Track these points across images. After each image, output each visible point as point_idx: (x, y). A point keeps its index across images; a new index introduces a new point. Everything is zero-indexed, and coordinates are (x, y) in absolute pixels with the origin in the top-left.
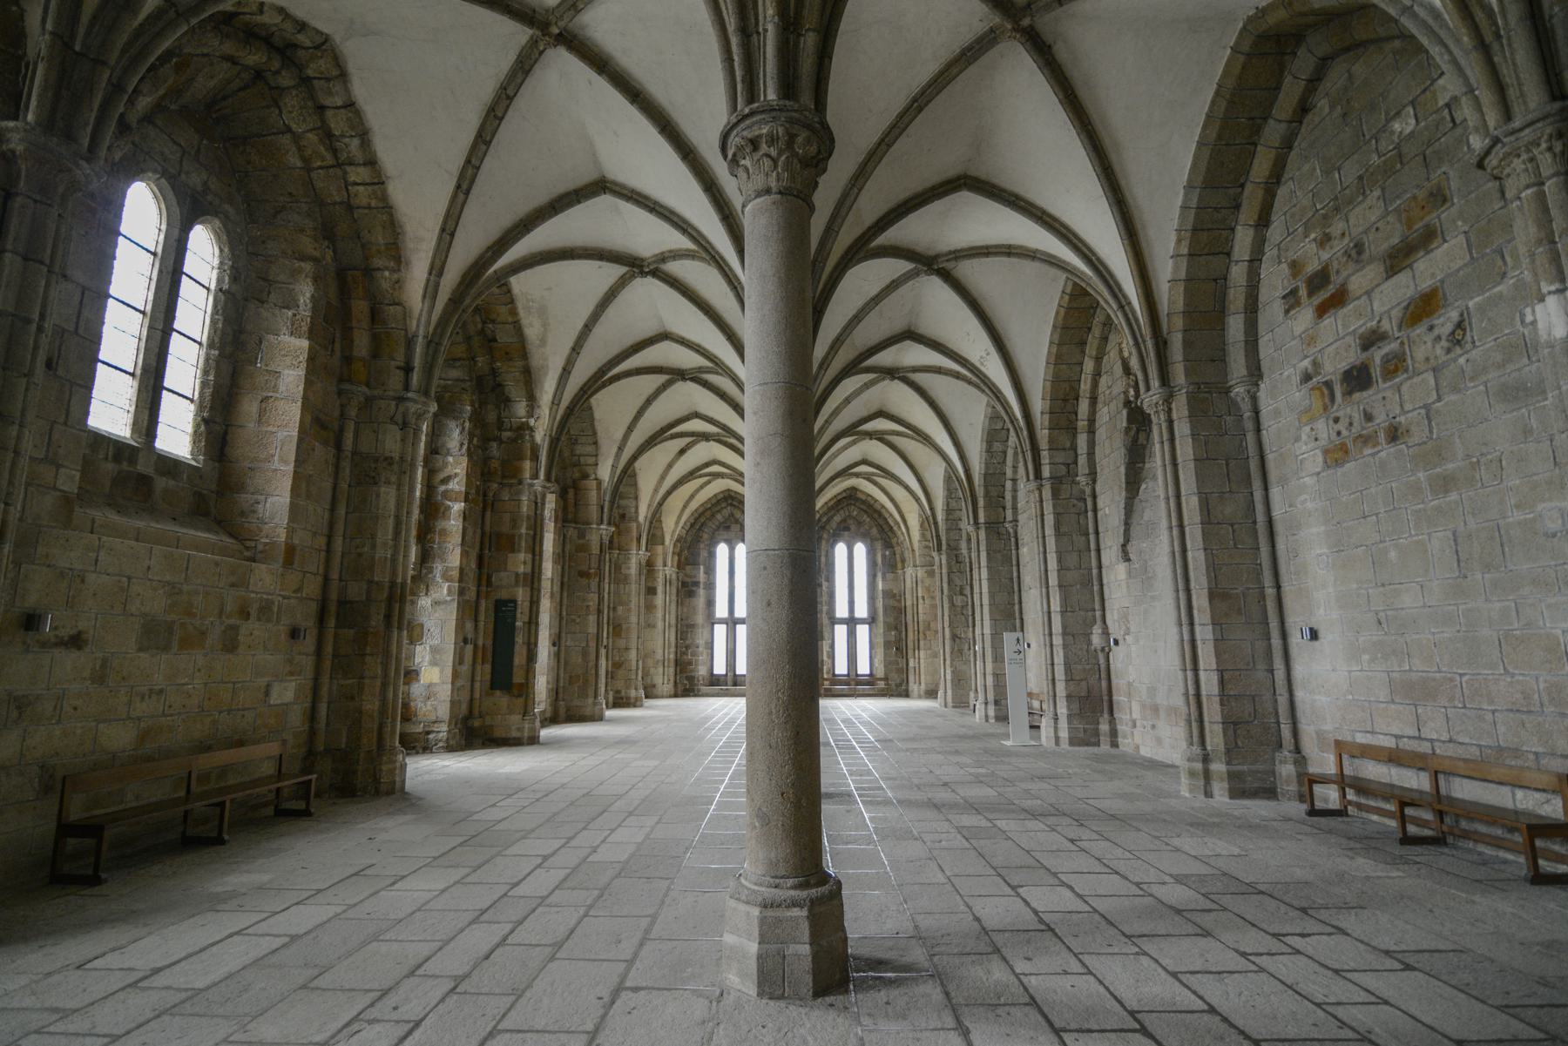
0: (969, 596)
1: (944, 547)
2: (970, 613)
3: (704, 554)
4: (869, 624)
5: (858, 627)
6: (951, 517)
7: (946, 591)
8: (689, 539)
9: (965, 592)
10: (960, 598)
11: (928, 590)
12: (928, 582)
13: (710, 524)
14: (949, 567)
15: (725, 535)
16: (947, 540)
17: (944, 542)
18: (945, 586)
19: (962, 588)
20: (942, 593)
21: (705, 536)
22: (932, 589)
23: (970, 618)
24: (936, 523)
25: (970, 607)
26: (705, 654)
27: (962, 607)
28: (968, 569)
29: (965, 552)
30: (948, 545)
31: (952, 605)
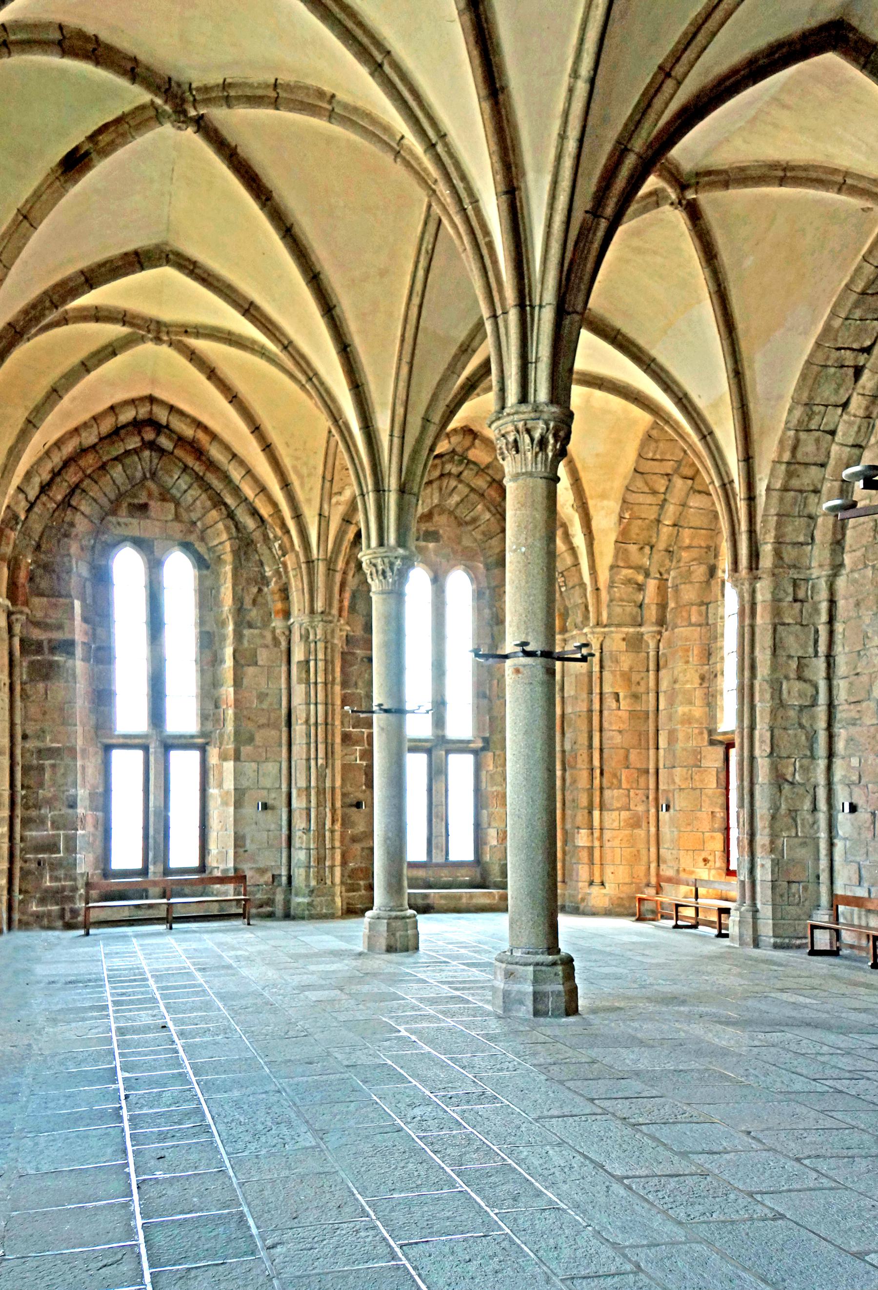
0: (822, 685)
1: (767, 561)
2: (822, 724)
3: (80, 569)
4: (476, 752)
5: (453, 758)
6: (795, 483)
7: (763, 670)
8: (37, 528)
9: (807, 674)
10: (797, 686)
11: (627, 677)
12: (626, 661)
13: (94, 491)
14: (777, 612)
15: (136, 526)
16: (779, 543)
17: (767, 550)
18: (763, 657)
19: (802, 664)
20: (753, 676)
21: (82, 525)
22: (635, 677)
23: (822, 737)
24: (751, 499)
25: (821, 711)
26: (90, 828)
27: (802, 708)
28: (824, 617)
29: (819, 573)
30: (778, 554)
31: (779, 704)
